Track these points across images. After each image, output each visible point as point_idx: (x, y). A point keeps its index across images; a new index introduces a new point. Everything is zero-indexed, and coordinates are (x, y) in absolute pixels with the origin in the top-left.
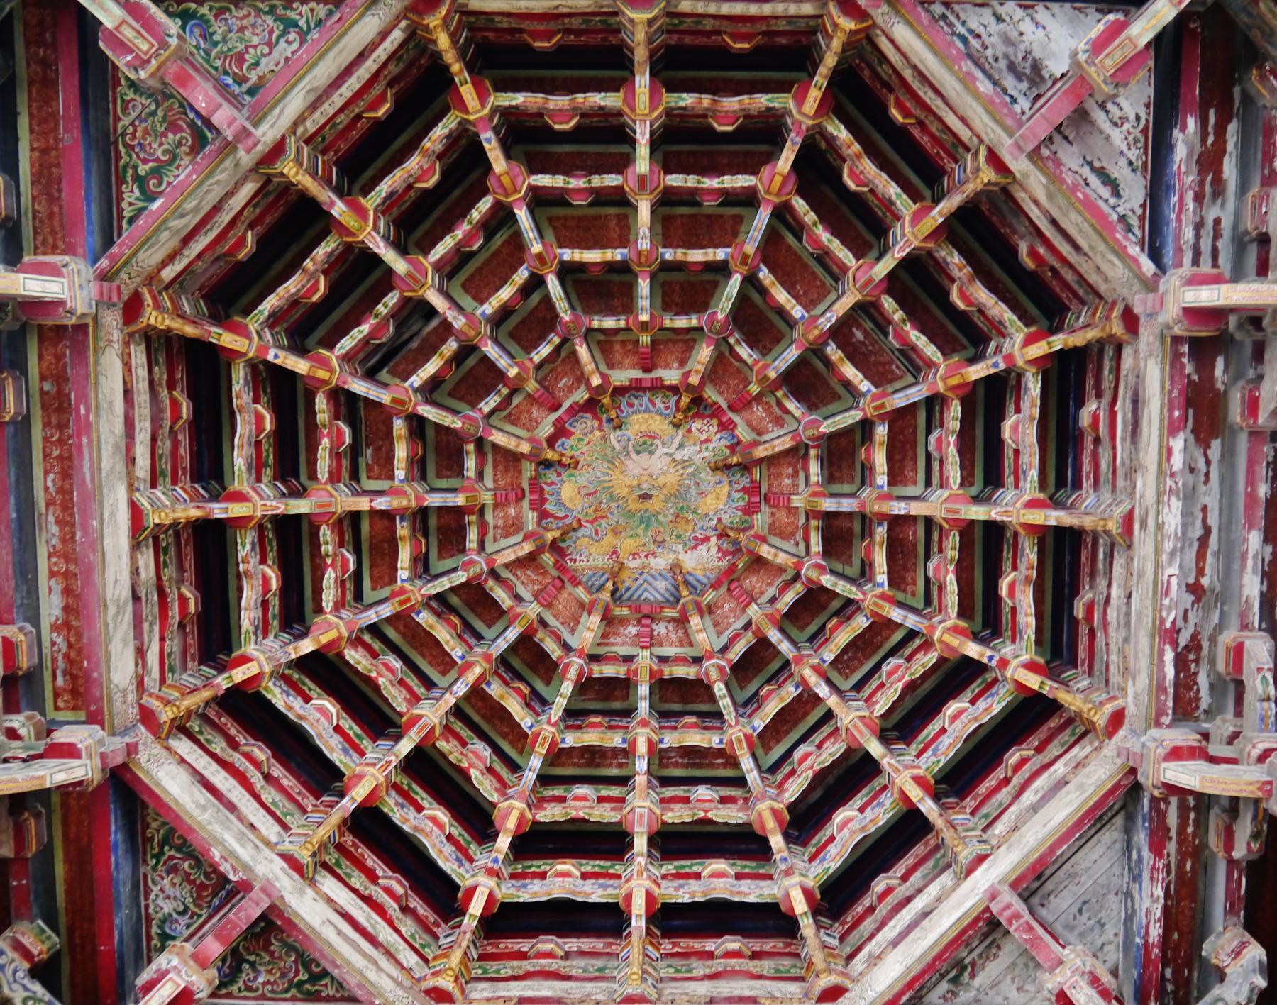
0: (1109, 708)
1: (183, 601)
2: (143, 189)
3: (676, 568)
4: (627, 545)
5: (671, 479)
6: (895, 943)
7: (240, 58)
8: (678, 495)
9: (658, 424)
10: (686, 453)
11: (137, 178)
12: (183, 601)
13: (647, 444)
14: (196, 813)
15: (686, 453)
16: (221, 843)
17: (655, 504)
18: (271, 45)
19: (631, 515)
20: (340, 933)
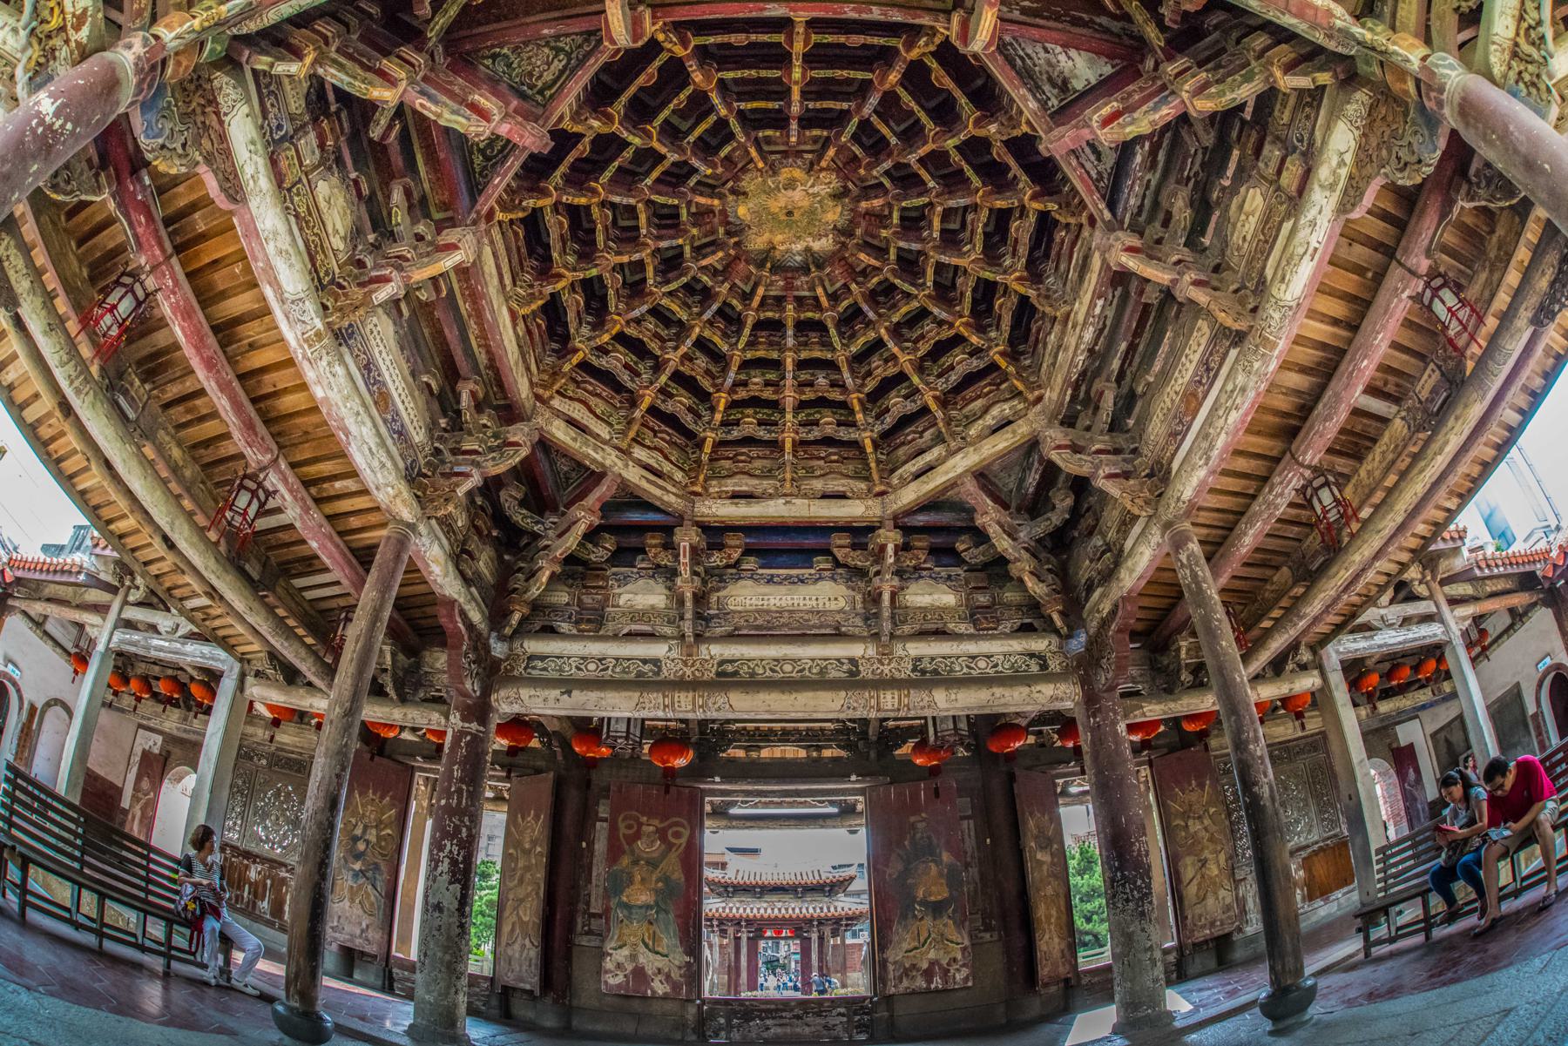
0: (1037, 393)
1: (539, 326)
2: (484, 155)
3: (808, 250)
4: (779, 238)
5: (806, 203)
6: (917, 476)
7: (530, 74)
8: (811, 213)
9: (798, 174)
10: (816, 189)
11: (479, 150)
12: (539, 326)
13: (791, 185)
14: (571, 443)
15: (816, 189)
16: (588, 456)
17: (797, 215)
18: (549, 64)
19: (780, 222)
20: (649, 481)
